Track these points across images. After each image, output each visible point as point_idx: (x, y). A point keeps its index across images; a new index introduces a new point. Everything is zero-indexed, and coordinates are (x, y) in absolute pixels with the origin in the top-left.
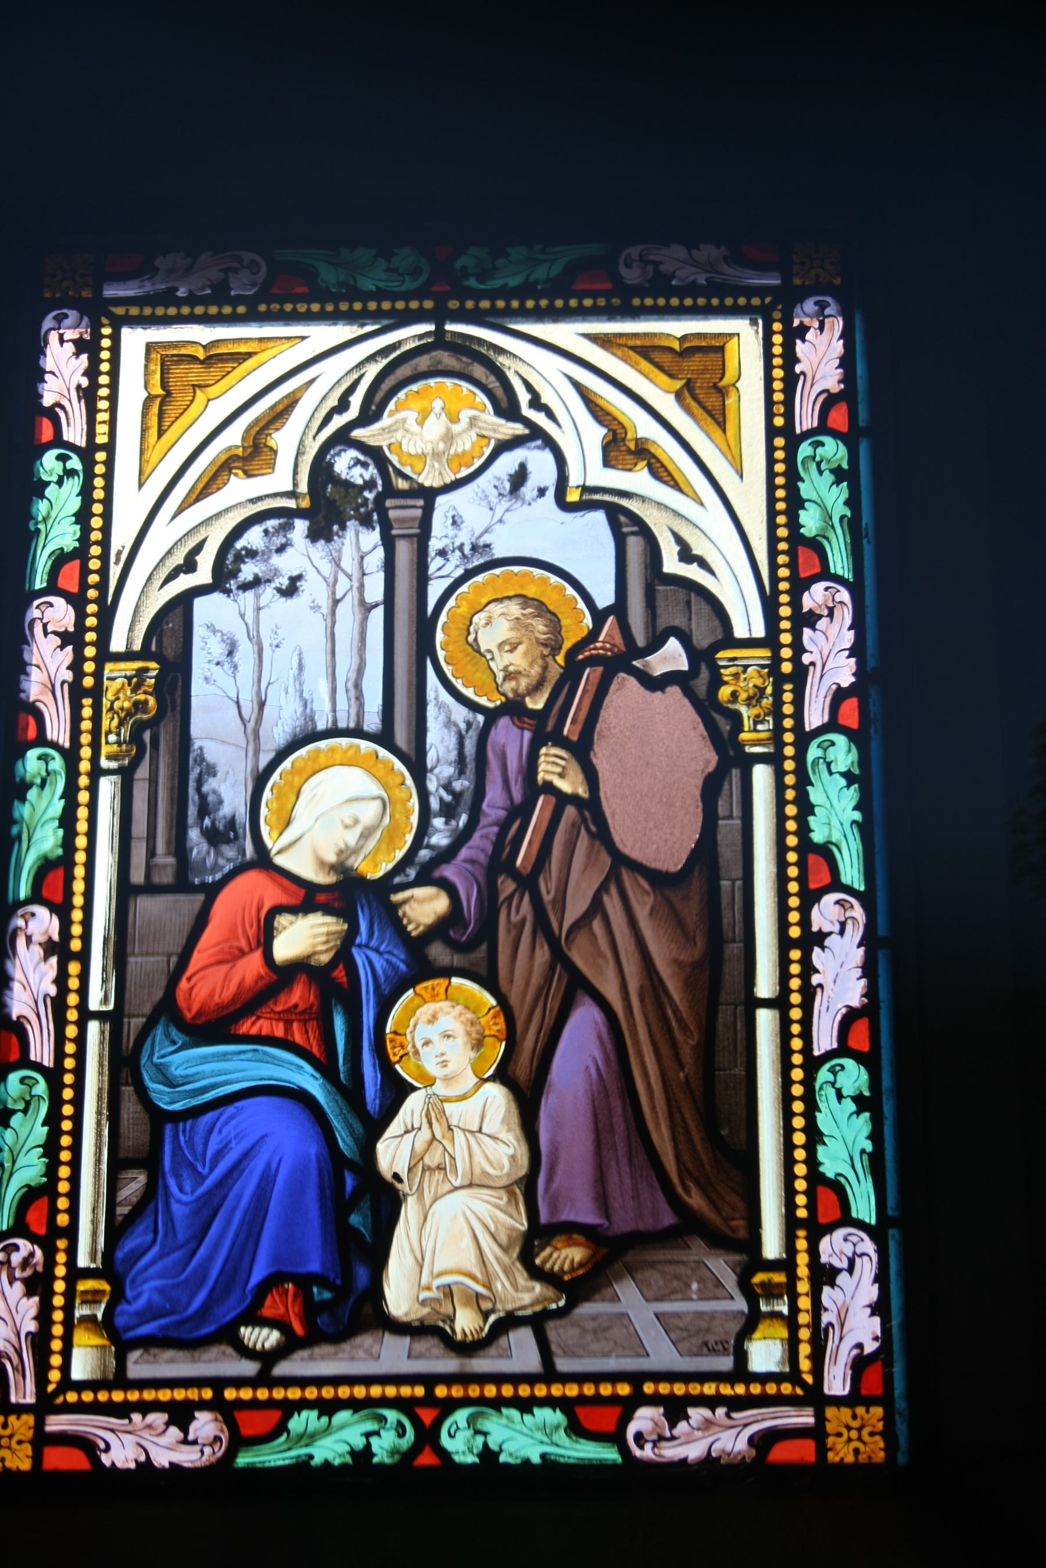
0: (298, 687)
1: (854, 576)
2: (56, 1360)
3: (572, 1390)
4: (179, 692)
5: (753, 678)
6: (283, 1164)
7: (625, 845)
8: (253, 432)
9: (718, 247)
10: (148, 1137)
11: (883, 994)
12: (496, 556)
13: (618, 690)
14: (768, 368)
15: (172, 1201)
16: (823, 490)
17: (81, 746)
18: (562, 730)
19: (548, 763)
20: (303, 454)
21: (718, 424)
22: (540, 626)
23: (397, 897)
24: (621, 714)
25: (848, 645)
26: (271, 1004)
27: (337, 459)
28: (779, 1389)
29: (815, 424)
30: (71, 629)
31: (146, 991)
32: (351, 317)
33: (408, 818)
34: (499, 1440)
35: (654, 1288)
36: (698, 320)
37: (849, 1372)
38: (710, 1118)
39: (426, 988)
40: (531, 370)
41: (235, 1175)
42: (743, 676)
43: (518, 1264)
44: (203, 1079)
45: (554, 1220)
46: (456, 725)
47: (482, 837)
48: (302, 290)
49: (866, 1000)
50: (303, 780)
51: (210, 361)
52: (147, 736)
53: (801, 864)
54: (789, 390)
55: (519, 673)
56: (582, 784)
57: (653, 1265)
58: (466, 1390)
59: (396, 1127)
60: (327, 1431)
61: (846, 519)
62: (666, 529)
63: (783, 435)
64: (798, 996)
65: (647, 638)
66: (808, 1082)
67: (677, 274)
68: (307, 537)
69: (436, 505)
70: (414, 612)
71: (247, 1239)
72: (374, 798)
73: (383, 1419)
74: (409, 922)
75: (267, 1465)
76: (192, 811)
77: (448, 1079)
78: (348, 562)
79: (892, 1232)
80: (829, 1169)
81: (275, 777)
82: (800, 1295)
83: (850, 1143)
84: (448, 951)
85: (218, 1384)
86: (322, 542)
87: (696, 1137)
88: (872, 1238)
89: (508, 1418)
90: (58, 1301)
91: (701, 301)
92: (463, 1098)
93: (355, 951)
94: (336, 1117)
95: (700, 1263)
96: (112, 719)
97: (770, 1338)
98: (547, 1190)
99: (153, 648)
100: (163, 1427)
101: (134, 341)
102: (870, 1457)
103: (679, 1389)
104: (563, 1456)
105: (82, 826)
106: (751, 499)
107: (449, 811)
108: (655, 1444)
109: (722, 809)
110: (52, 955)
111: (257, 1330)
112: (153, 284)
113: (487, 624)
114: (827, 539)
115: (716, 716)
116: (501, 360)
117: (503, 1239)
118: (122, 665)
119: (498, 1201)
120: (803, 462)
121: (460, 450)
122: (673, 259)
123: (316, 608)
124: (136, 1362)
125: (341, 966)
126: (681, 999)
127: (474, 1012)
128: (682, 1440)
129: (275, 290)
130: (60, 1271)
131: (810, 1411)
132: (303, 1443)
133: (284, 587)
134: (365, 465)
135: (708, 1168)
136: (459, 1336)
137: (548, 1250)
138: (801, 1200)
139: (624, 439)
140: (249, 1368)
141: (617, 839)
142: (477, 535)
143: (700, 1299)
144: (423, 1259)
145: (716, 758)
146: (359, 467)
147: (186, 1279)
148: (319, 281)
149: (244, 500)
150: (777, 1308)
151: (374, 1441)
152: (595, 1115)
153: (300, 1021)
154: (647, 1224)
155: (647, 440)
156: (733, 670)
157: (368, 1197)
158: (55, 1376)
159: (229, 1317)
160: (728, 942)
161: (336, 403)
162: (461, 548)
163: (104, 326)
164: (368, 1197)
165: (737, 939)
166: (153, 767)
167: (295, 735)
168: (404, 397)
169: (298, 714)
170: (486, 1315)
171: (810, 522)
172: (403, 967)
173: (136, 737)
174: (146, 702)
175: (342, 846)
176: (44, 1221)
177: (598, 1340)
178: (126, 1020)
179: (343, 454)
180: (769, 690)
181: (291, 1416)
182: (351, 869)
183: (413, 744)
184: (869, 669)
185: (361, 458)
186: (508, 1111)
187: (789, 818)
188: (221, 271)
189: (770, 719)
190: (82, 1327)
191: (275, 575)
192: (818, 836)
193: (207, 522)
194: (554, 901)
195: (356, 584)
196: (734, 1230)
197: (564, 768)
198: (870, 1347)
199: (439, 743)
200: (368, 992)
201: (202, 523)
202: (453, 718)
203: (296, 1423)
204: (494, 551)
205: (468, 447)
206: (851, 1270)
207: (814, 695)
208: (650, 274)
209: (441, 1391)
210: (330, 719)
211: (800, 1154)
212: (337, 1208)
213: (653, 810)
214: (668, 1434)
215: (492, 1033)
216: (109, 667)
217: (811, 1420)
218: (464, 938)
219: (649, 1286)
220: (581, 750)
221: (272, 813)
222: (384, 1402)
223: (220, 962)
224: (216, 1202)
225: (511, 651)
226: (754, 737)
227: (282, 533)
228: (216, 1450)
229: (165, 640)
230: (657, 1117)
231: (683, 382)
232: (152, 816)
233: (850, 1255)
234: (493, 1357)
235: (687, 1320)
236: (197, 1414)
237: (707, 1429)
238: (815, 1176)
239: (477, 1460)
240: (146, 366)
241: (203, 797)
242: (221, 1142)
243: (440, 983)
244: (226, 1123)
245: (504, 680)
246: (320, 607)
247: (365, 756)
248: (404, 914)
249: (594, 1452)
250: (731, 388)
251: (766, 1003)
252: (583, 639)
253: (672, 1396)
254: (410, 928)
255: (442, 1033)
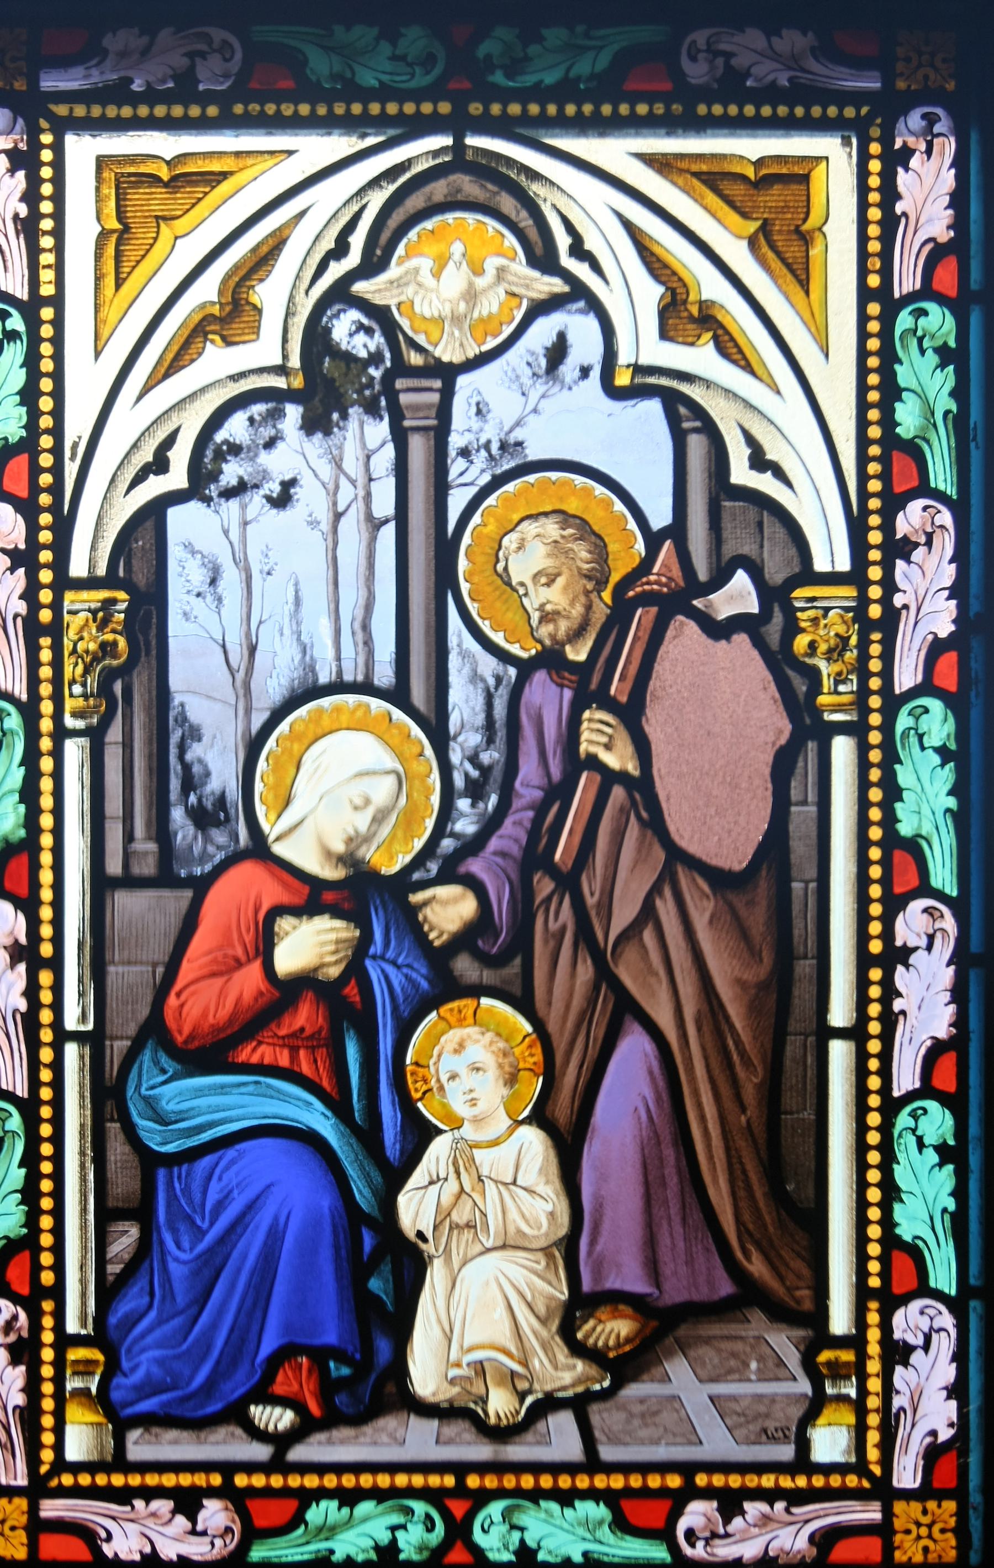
0: (294, 627)
1: (958, 493)
2: (48, 1438)
3: (617, 1482)
4: (153, 632)
5: (836, 625)
6: (291, 1219)
7: (682, 837)
8: (232, 284)
9: (805, 34)
10: (139, 1183)
11: (974, 1023)
12: (530, 458)
13: (675, 637)
14: (863, 206)
15: (169, 1259)
16: (925, 376)
17: (41, 699)
18: (609, 690)
19: (592, 730)
20: (294, 314)
21: (800, 282)
22: (582, 552)
23: (417, 898)
24: (679, 669)
25: (948, 583)
26: (273, 1026)
27: (335, 322)
28: (844, 1482)
29: (918, 286)
30: (22, 546)
31: (130, 1007)
32: (349, 124)
33: (428, 798)
34: (537, 1538)
35: (709, 1367)
36: (777, 137)
37: (921, 1463)
38: (774, 1169)
39: (451, 1010)
40: (572, 203)
41: (239, 1230)
42: (824, 620)
43: (558, 1339)
44: (198, 1115)
45: (598, 1288)
46: (483, 680)
47: (514, 823)
48: (288, 84)
49: (954, 1031)
50: (304, 747)
51: (178, 182)
52: (118, 687)
53: (886, 862)
54: (888, 239)
55: (557, 613)
56: (632, 758)
57: (708, 1341)
58: (500, 1481)
59: (418, 1177)
60: (349, 1523)
61: (951, 416)
62: (735, 425)
63: (879, 299)
64: (878, 1024)
65: (710, 570)
66: (886, 1129)
67: (753, 70)
68: (301, 428)
69: (457, 388)
70: (432, 531)
71: (255, 1304)
72: (388, 773)
73: (409, 1512)
74: (431, 929)
75: (284, 1560)
76: (175, 784)
77: (477, 1121)
78: (352, 464)
79: (974, 1304)
80: (906, 1231)
81: (271, 743)
82: (869, 1376)
83: (930, 1201)
84: (476, 965)
85: (228, 1469)
86: (319, 435)
87: (759, 1192)
88: (951, 1311)
89: (546, 1511)
90: (47, 1371)
91: (782, 110)
92: (495, 1143)
93: (368, 963)
94: (351, 1163)
95: (760, 1338)
96: (76, 664)
97: (836, 1424)
98: (590, 1253)
99: (121, 573)
100: (169, 1516)
101: (82, 151)
102: (940, 1557)
103: (735, 1481)
104: (608, 1555)
105: (47, 802)
106: (837, 384)
107: (475, 791)
108: (707, 1541)
109: (795, 793)
110: (20, 961)
111: (269, 1409)
112: (102, 73)
113: (519, 548)
114: (927, 441)
115: (791, 673)
116: (535, 188)
117: (542, 1310)
118: (85, 595)
119: (535, 1265)
120: (901, 338)
121: (485, 313)
122: (747, 47)
123: (314, 524)
124: (136, 1443)
125: (353, 982)
126: (743, 1028)
127: (507, 1041)
128: (737, 1537)
129: (254, 85)
130: (48, 1337)
131: (877, 1505)
132: (322, 1536)
133: (275, 495)
134: (369, 331)
135: (771, 1229)
136: (493, 1420)
137: (591, 1323)
138: (874, 1267)
139: (685, 302)
140: (262, 1452)
141: (672, 828)
142: (506, 429)
143: (759, 1380)
144: (452, 1331)
145: (790, 727)
146: (362, 333)
147: (188, 1349)
148: (308, 72)
149: (223, 376)
150: (844, 1391)
151: (400, 1535)
152: (645, 1166)
153: (307, 1047)
154: (702, 1294)
155: (713, 303)
156: (811, 613)
157: (389, 1258)
158: (47, 1455)
159: (237, 1394)
160: (799, 958)
161: (332, 245)
162: (487, 446)
163: (43, 131)
164: (389, 1258)
165: (810, 955)
166: (127, 728)
167: (293, 690)
168: (415, 239)
169: (296, 662)
170: (522, 1396)
171: (908, 418)
172: (424, 984)
173: (105, 689)
174: (115, 643)
175: (352, 833)
176: (27, 1278)
177: (646, 1425)
178: (108, 1043)
179: (342, 315)
180: (854, 640)
181: (308, 1506)
182: (362, 861)
183: (433, 704)
184: (971, 614)
185: (365, 321)
186: (546, 1159)
187: (873, 805)
188: (185, 55)
189: (854, 677)
190: (76, 1400)
191: (264, 478)
192: (905, 829)
193: (179, 405)
194: (599, 904)
195: (361, 493)
196: (798, 1302)
197: (611, 737)
198: (945, 1434)
199: (464, 704)
200: (384, 1014)
201: (174, 406)
202: (479, 671)
203: (315, 1514)
204: (527, 451)
205: (495, 309)
206: (926, 1347)
207: (906, 648)
208: (720, 71)
209: (473, 1481)
210: (334, 670)
211: (874, 1214)
212: (356, 1270)
213: (715, 793)
214: (722, 1531)
215: (528, 1066)
216: (69, 596)
217: (878, 1516)
218: (495, 950)
219: (704, 1364)
220: (631, 715)
221: (269, 789)
222: (411, 1492)
223: (213, 975)
224: (218, 1260)
225: (548, 585)
226: (834, 702)
227: (270, 423)
228: (228, 1542)
229: (134, 562)
230: (714, 1169)
231: (759, 223)
232: (127, 791)
233: (926, 1330)
234: (529, 1444)
235: (744, 1403)
236: (206, 1502)
237: (765, 1525)
238: (890, 1240)
239: (513, 1558)
240: (98, 189)
241: (187, 768)
242: (221, 1191)
243: (467, 1004)
244: (227, 1168)
245: (540, 622)
246: (319, 523)
247: (376, 718)
248: (425, 919)
249: (641, 1551)
250: (817, 234)
251: (841, 1033)
252: (634, 570)
253: (727, 1490)
254: (432, 936)
255: (470, 1066)
